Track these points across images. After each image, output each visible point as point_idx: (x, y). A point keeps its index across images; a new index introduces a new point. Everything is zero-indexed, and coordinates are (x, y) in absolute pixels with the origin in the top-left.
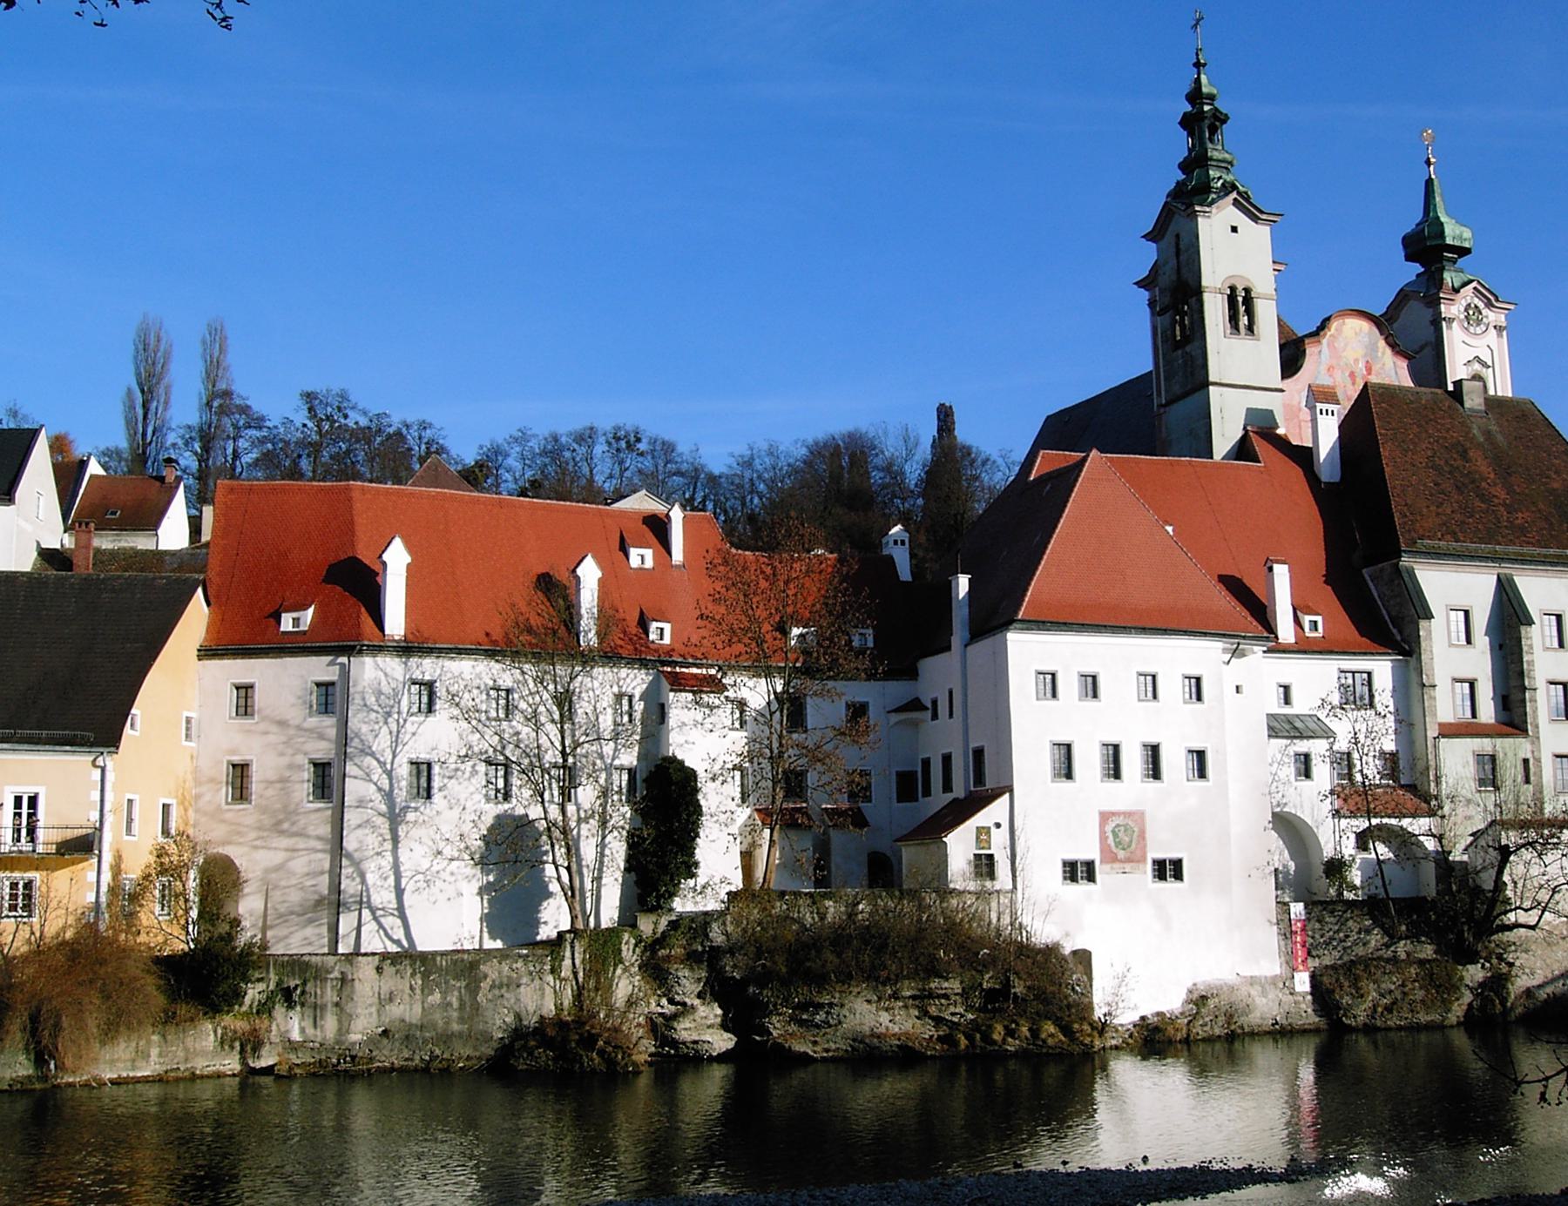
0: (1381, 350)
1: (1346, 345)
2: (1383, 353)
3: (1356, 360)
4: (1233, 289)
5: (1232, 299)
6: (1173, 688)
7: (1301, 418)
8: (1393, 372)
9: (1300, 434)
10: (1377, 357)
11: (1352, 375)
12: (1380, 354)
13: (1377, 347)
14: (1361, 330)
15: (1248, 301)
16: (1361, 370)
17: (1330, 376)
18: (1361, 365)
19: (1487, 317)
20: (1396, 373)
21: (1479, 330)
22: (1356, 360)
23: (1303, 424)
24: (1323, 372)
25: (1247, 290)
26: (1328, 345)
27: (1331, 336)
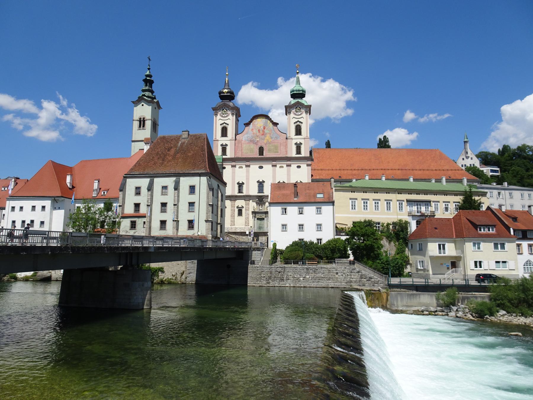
1: (258, 123)
2: (269, 124)
4: (140, 118)
5: (140, 121)
6: (39, 208)
8: (272, 128)
9: (242, 146)
11: (259, 131)
12: (268, 124)
15: (144, 121)
18: (262, 127)
21: (299, 114)
25: (144, 118)
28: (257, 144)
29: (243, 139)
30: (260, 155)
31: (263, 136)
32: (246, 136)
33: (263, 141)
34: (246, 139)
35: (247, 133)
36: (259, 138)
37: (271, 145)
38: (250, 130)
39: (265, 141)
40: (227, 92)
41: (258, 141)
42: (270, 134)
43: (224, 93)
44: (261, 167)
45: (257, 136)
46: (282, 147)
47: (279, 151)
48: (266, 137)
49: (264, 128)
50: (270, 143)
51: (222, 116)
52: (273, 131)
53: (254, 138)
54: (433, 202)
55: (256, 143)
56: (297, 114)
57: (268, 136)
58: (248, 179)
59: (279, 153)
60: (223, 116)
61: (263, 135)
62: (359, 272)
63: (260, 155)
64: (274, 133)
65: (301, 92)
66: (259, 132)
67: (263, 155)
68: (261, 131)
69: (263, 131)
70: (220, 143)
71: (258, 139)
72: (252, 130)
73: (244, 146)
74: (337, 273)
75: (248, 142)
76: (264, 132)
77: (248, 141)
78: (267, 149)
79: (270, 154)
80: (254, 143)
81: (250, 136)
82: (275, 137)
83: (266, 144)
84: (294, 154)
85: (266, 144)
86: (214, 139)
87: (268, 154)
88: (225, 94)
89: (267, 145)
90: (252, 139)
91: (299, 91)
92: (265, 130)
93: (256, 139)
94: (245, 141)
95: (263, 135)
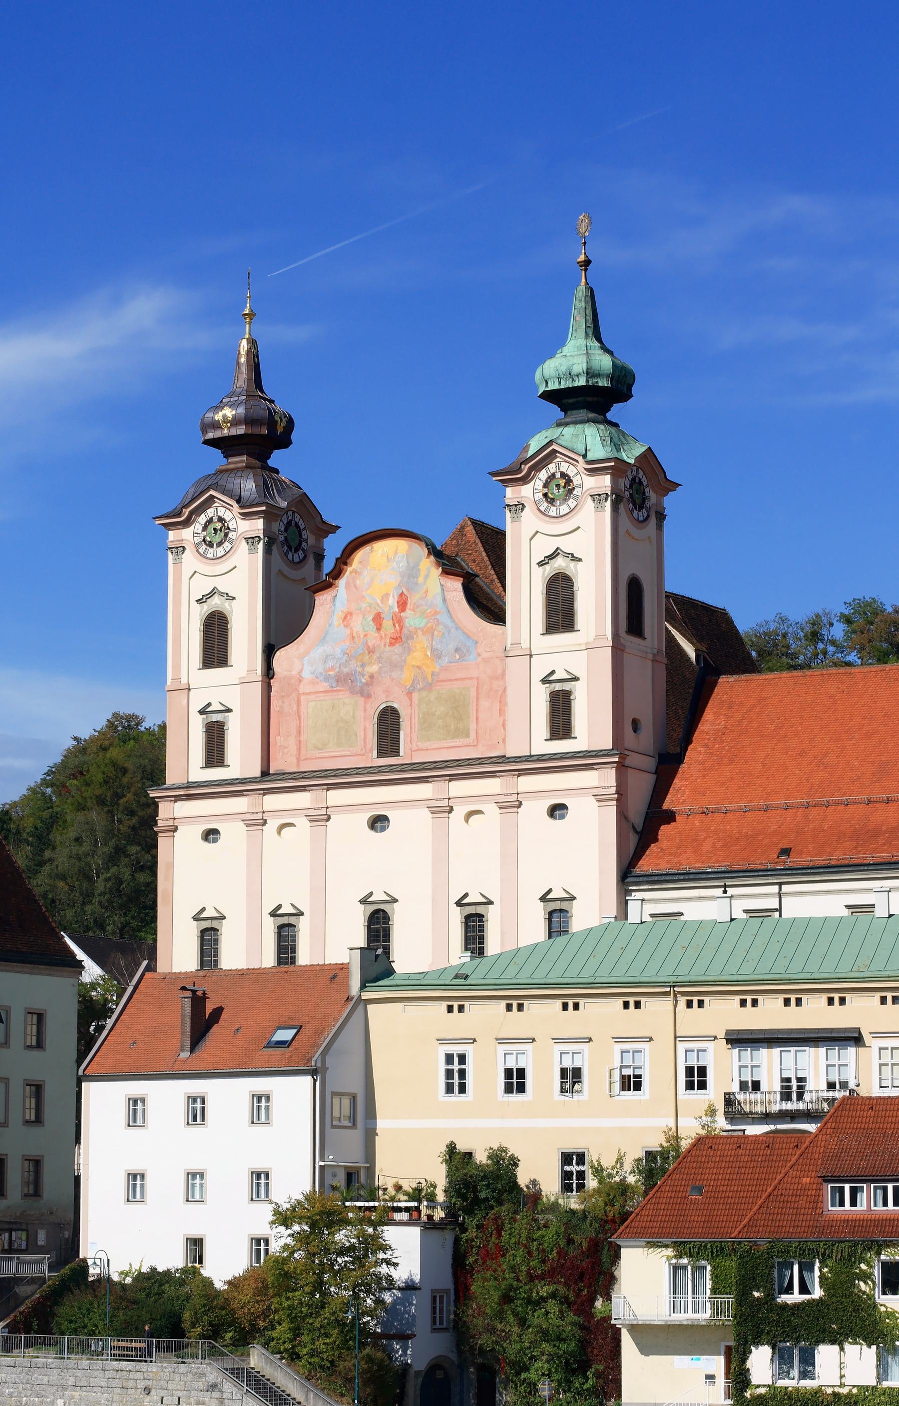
0: (423, 573)
2: (427, 577)
3: (386, 596)
7: (301, 691)
8: (439, 600)
9: (298, 711)
10: (417, 584)
11: (378, 619)
12: (421, 580)
13: (419, 570)
14: (396, 553)
16: (391, 607)
17: (346, 626)
18: (392, 602)
19: (581, 486)
20: (444, 600)
21: (564, 509)
22: (386, 596)
23: (302, 697)
24: (336, 623)
26: (347, 585)
27: (351, 573)
28: (369, 696)
29: (307, 675)
30: (381, 753)
31: (397, 649)
32: (318, 652)
33: (394, 675)
34: (320, 669)
35: (323, 639)
36: (379, 659)
37: (432, 696)
38: (337, 619)
39: (407, 676)
40: (235, 422)
41: (372, 677)
42: (429, 631)
43: (215, 425)
44: (378, 822)
45: (371, 651)
46: (484, 703)
47: (473, 727)
48: (409, 650)
49: (403, 604)
50: (429, 687)
51: (204, 556)
52: (444, 618)
53: (354, 665)
54: (876, 1035)
55: (364, 693)
56: (553, 511)
57: (421, 642)
58: (320, 889)
59: (473, 735)
60: (211, 553)
61: (396, 640)
62: (213, 1387)
63: (381, 753)
64: (450, 624)
65: (582, 382)
66: (379, 629)
67: (396, 752)
68: (387, 624)
69: (398, 621)
70: (197, 702)
71: (374, 668)
72: (347, 617)
73: (309, 707)
74: (148, 1391)
75: (324, 686)
76: (401, 628)
77: (327, 678)
78: (416, 721)
79: (427, 745)
80: (353, 693)
81: (338, 653)
82: (452, 646)
83: (409, 694)
84: (542, 745)
85: (409, 694)
86: (169, 683)
87: (421, 745)
88: (226, 432)
89: (415, 696)
90: (346, 670)
91: (571, 375)
92: (408, 613)
93: (363, 666)
94: (313, 683)
95: (396, 640)
